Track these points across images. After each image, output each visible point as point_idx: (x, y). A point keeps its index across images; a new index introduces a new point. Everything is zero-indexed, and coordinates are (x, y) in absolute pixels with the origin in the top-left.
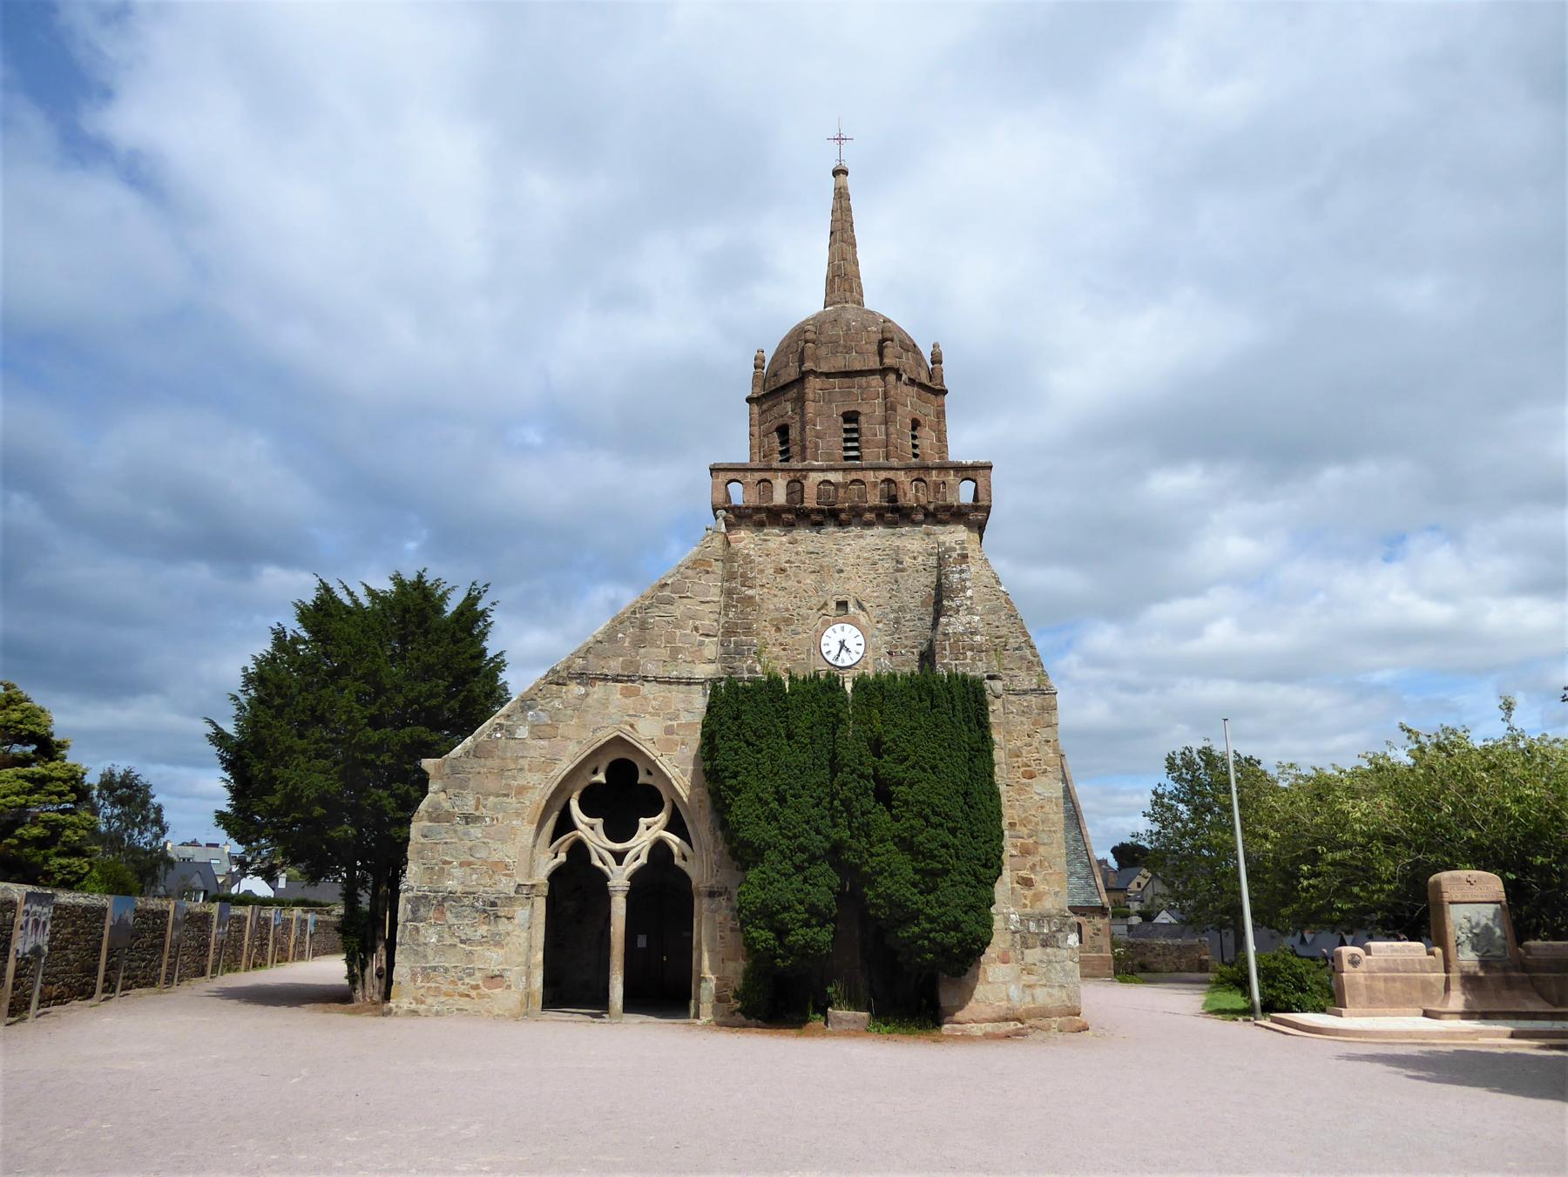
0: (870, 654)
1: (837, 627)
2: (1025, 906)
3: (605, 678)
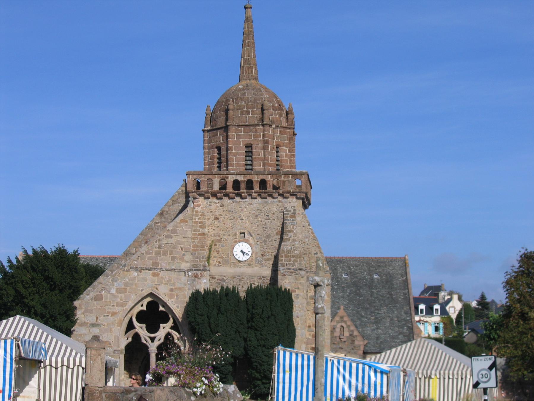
0: (254, 255)
1: (240, 244)
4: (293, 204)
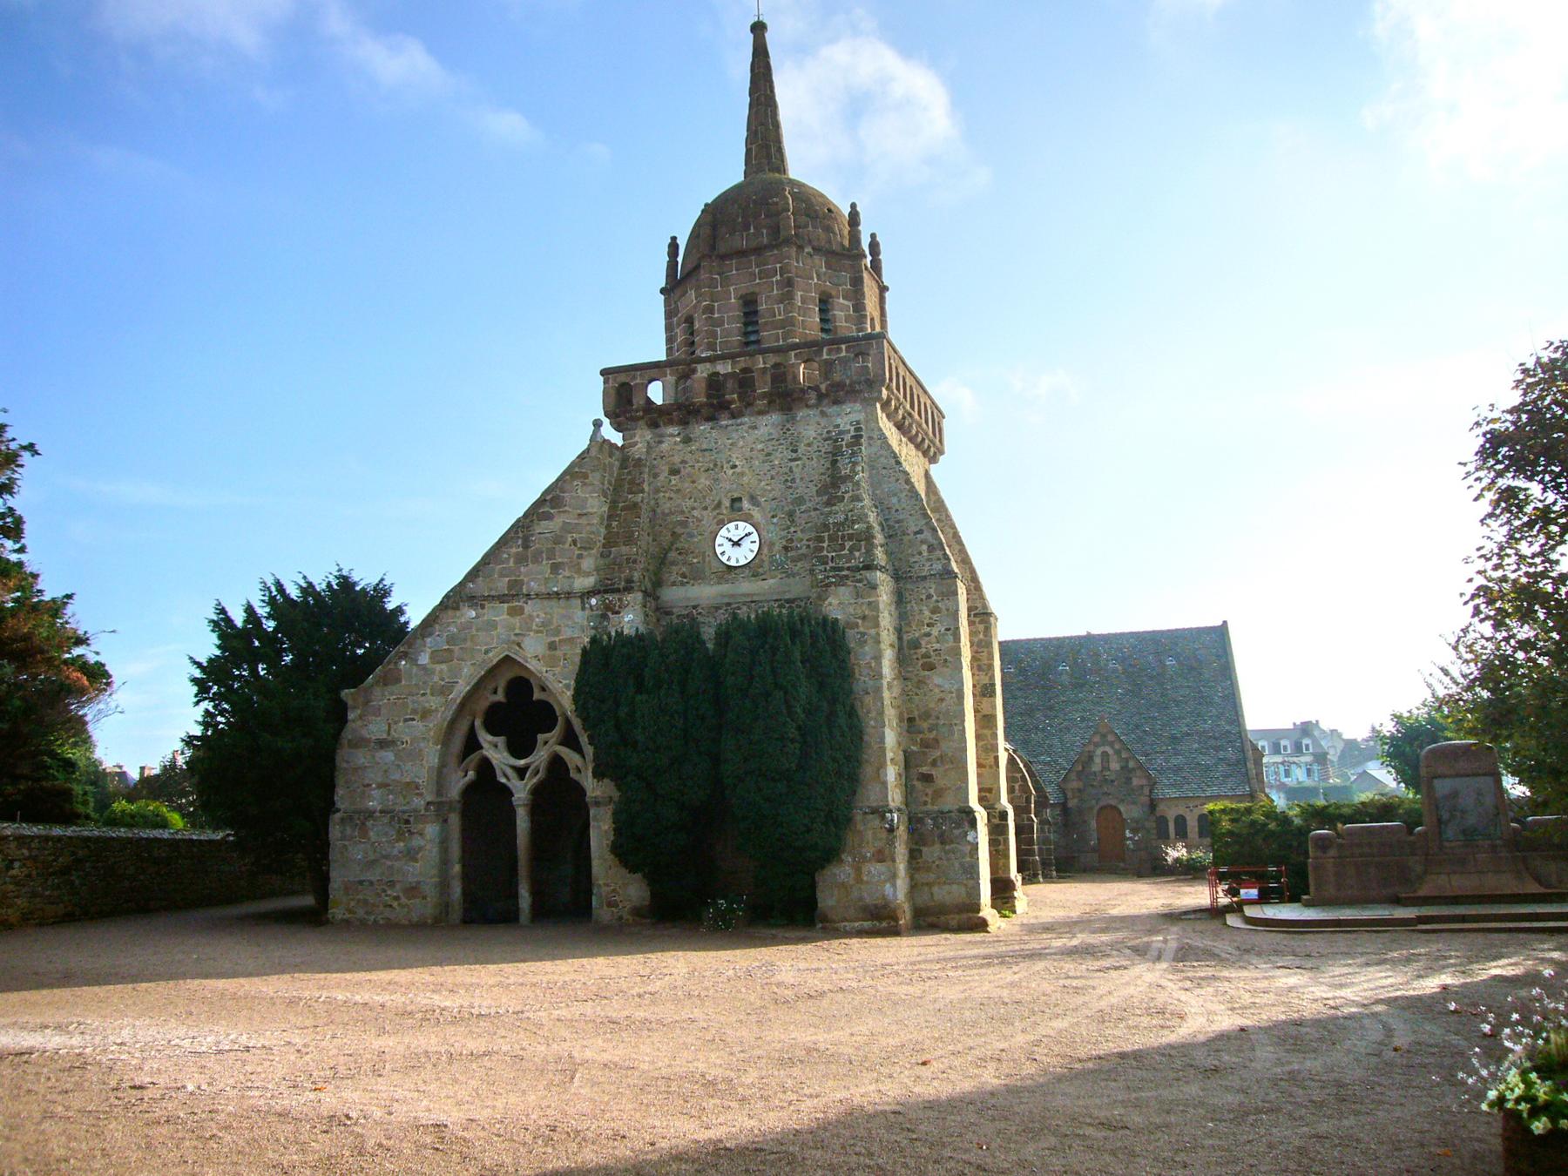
2: (925, 803)
3: (491, 598)
4: (854, 417)
